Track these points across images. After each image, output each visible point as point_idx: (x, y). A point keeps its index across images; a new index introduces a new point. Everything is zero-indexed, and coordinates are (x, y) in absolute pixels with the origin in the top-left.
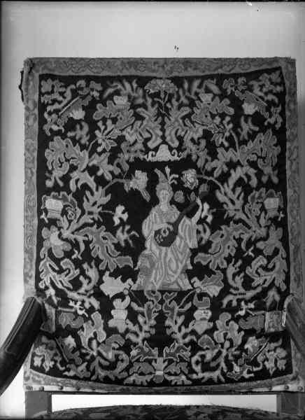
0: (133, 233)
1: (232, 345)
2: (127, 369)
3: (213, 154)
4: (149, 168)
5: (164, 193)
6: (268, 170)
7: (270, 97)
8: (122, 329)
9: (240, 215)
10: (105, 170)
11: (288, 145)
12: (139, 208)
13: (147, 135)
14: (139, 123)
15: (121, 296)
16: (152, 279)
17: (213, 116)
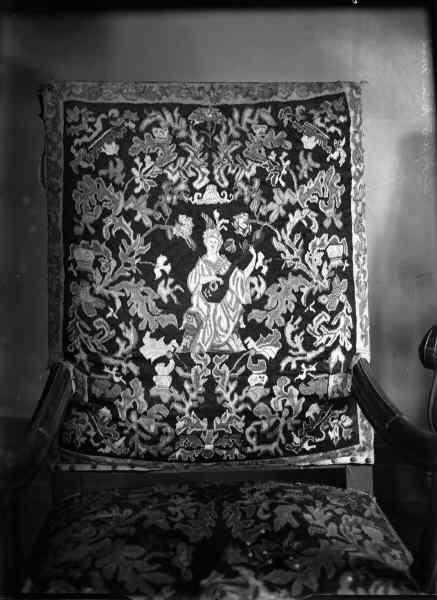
0: (177, 287)
1: (291, 415)
2: (172, 444)
3: (269, 197)
5: (212, 240)
6: (330, 212)
7: (332, 129)
8: (165, 400)
9: (299, 266)
10: (143, 215)
11: (353, 182)
12: (185, 258)
13: (191, 174)
14: (182, 159)
15: (164, 360)
16: (200, 340)
17: (268, 152)
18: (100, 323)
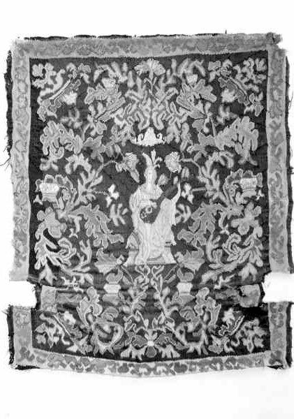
4: (137, 150)
5: (150, 173)
18: (64, 243)
